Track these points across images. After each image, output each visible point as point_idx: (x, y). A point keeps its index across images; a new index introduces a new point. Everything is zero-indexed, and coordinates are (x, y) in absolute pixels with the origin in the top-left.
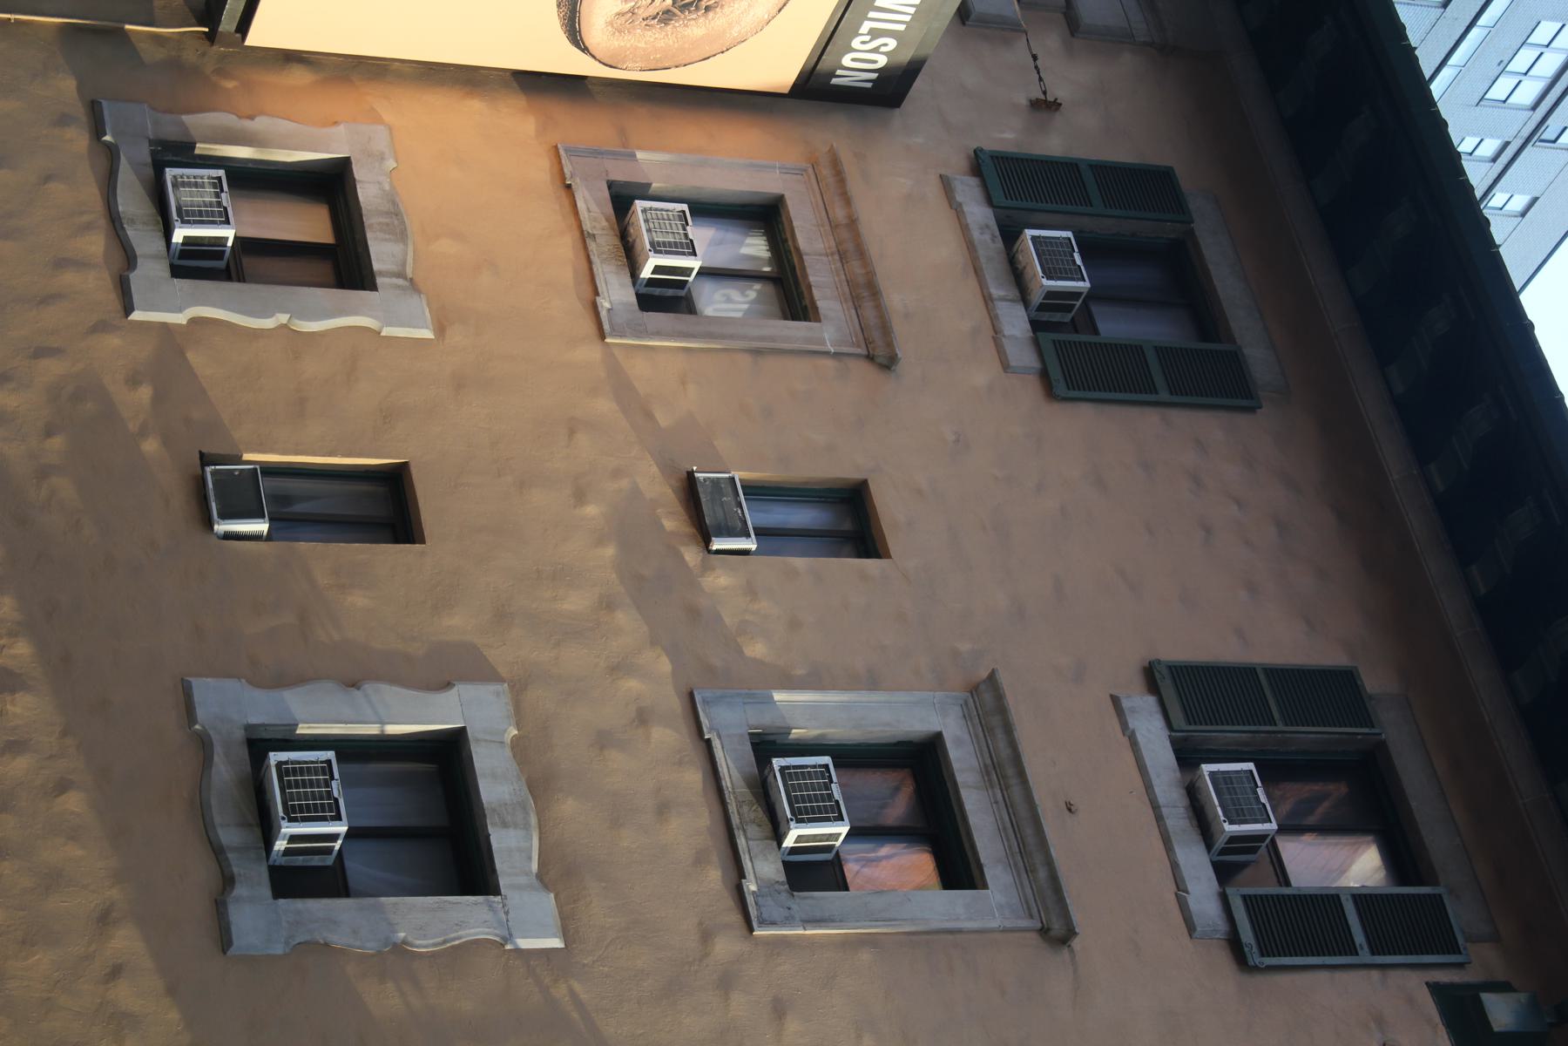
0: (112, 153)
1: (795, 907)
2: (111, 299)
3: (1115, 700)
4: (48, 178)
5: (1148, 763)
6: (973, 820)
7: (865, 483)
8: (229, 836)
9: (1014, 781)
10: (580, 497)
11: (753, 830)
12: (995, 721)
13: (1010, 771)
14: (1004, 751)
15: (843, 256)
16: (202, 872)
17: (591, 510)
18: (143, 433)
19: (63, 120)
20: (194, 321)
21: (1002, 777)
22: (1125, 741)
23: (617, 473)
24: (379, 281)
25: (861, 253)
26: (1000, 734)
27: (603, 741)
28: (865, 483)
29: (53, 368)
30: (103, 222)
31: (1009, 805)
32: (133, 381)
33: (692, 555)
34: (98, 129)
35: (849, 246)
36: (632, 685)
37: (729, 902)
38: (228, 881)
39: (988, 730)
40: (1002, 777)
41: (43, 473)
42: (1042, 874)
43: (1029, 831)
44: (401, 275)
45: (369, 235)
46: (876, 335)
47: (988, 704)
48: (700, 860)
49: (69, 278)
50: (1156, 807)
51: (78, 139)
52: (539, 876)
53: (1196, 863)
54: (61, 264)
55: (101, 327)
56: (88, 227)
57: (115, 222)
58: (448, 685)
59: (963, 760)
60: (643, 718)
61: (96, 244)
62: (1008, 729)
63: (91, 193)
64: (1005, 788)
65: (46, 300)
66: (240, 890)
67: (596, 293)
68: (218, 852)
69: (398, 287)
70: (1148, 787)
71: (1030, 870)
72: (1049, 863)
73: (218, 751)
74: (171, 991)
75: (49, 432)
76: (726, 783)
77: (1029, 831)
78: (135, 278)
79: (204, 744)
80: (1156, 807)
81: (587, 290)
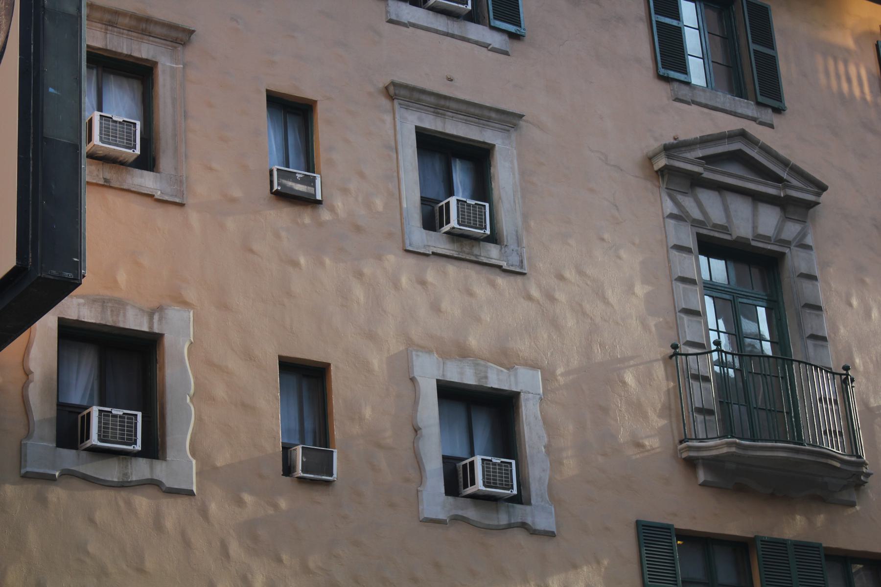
0: (68, 474)
1: (512, 247)
2: (181, 502)
3: (391, 21)
4: (92, 521)
5: (425, 25)
6: (455, 133)
7: (315, 102)
8: (503, 519)
9: (448, 103)
10: (295, 264)
11: (476, 251)
12: (416, 95)
13: (442, 102)
14: (432, 100)
15: (111, 24)
16: (520, 536)
17: (302, 261)
18: (276, 506)
19: (42, 500)
20: (193, 454)
21: (442, 107)
22: (411, 29)
23: (277, 236)
24: (156, 330)
25: (116, 13)
26: (424, 97)
27: (436, 308)
28: (315, 102)
29: (235, 548)
30: (124, 493)
31: (457, 112)
32: (240, 503)
33: (325, 215)
34: (51, 479)
35: (107, 17)
36: (404, 280)
37: (512, 278)
38: (524, 526)
39: (418, 101)
40: (442, 107)
41: (306, 570)
42: (493, 115)
43: (472, 110)
44: (151, 315)
45: (121, 325)
46: (174, 34)
47: (400, 94)
48: (493, 284)
49: (169, 524)
50: (447, 34)
51: (57, 494)
52: (508, 369)
53: (476, 31)
54: (158, 526)
55: (204, 512)
56: (129, 503)
57: (123, 485)
58: (413, 380)
59: (432, 123)
60: (423, 283)
61: (142, 502)
62: (423, 92)
63: (100, 496)
64: (448, 109)
65: (187, 543)
66: (529, 521)
67: (151, 196)
68: (510, 526)
69: (160, 320)
70: (437, 32)
71: (489, 119)
72: (491, 109)
73: (460, 513)
74: (575, 567)
75: (280, 561)
76: (448, 253)
77: (472, 110)
78: (169, 483)
79: (456, 519)
80: (447, 34)
81: (148, 200)
